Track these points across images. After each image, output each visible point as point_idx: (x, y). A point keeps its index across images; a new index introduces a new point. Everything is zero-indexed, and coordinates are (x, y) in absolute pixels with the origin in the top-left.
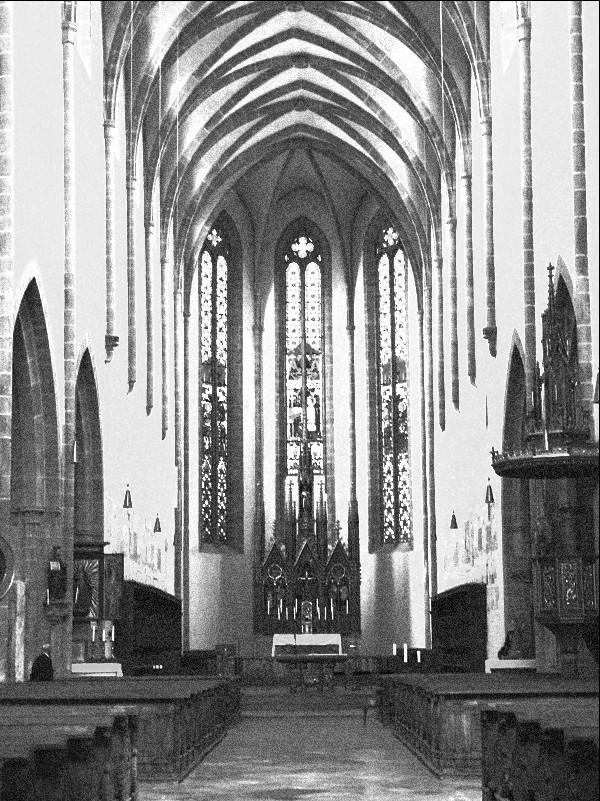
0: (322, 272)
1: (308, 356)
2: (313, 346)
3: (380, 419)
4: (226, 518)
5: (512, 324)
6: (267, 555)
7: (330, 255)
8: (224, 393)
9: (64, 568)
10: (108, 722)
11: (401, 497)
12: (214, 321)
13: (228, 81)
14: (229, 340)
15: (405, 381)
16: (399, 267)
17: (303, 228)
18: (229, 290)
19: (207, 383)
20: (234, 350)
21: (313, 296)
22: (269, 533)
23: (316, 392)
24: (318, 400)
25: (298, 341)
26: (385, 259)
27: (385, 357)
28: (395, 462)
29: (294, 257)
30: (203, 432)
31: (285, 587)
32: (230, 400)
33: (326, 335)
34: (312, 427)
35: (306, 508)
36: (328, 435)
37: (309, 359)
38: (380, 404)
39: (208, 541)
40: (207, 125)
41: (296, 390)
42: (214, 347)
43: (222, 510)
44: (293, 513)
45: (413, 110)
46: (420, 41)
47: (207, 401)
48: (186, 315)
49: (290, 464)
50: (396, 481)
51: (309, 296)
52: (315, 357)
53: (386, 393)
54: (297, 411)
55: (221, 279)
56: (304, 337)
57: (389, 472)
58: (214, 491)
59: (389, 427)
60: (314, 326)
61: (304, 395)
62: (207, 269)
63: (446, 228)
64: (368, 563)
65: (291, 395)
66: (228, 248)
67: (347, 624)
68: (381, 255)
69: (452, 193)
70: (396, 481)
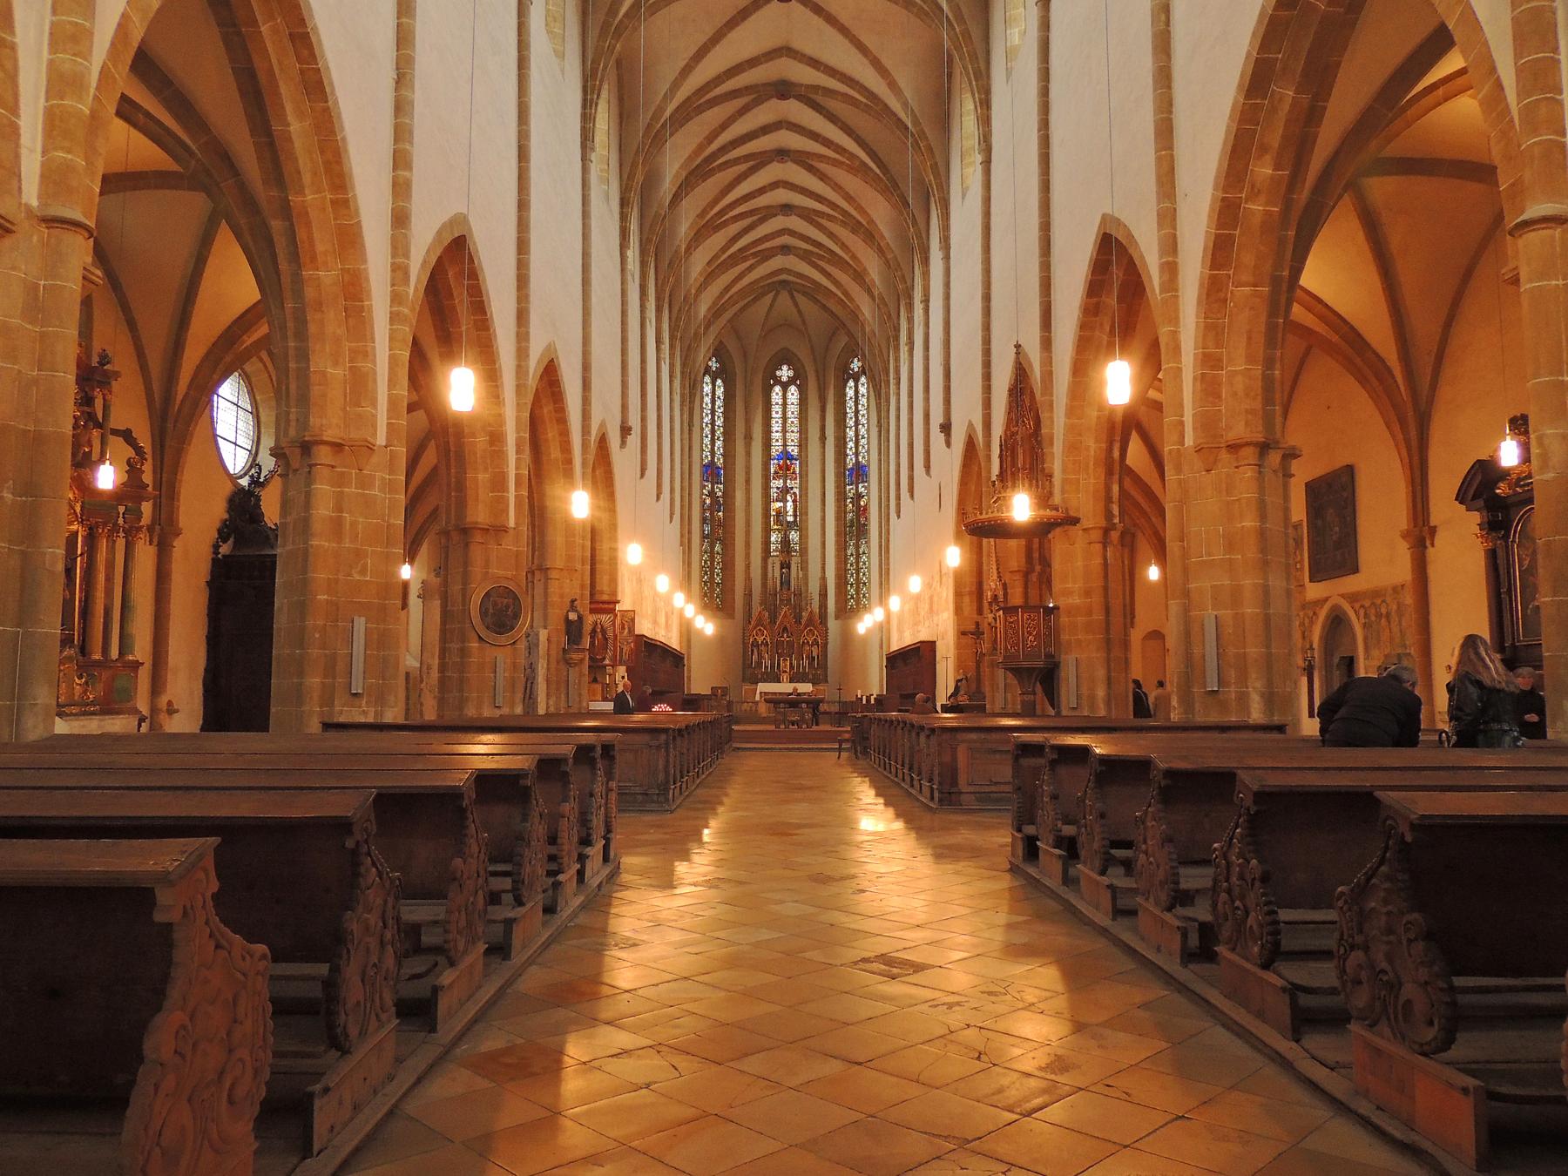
5: (967, 412)
9: (580, 617)
10: (567, 750)
12: (713, 432)
13: (725, 224)
16: (862, 390)
17: (785, 358)
18: (725, 406)
26: (851, 383)
27: (850, 461)
29: (778, 381)
30: (704, 521)
34: (790, 519)
40: (709, 263)
42: (713, 453)
44: (774, 583)
45: (881, 251)
46: (890, 186)
49: (773, 547)
56: (785, 445)
58: (712, 568)
60: (793, 436)
62: (707, 389)
63: (904, 349)
64: (832, 624)
65: (774, 493)
66: (725, 373)
67: (818, 674)
69: (910, 320)
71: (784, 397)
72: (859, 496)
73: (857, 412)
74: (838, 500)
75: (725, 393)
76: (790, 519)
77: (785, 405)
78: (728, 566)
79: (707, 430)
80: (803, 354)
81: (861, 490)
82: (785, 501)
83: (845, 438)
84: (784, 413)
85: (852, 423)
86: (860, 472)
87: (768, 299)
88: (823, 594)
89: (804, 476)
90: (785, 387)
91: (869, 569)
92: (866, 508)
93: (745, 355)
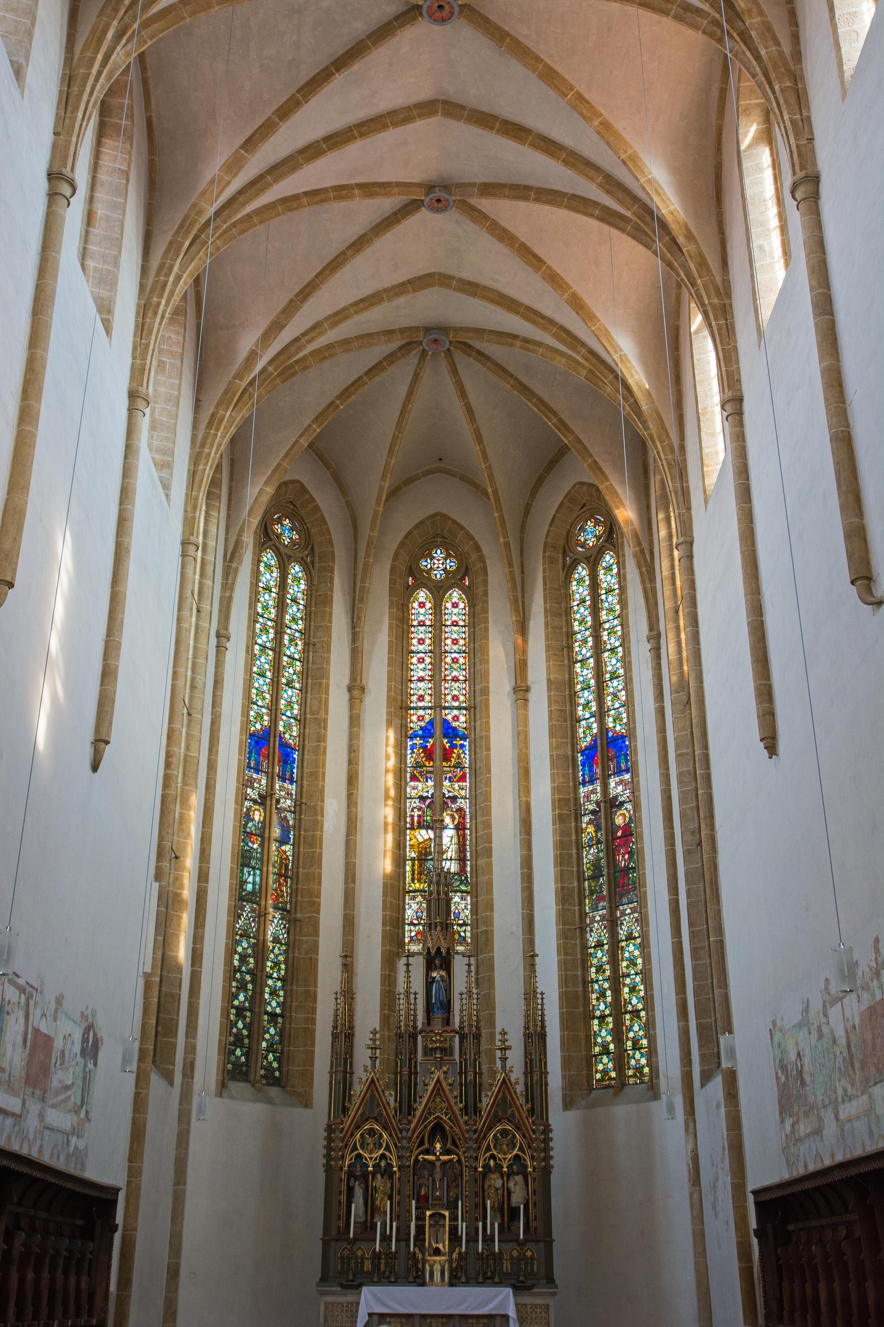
0: (472, 604)
1: (445, 741)
2: (455, 724)
3: (580, 847)
4: (281, 1033)
6: (356, 1101)
7: (486, 574)
8: (289, 794)
12: (277, 667)
14: (303, 704)
15: (627, 771)
16: (607, 580)
17: (439, 533)
18: (309, 616)
19: (257, 771)
20: (312, 719)
21: (455, 642)
22: (362, 1056)
23: (461, 803)
24: (464, 819)
25: (428, 715)
26: (582, 571)
28: (613, 924)
29: (422, 580)
30: (244, 859)
31: (391, 1175)
32: (299, 807)
33: (476, 707)
34: (453, 867)
35: (439, 1006)
36: (483, 878)
37: (447, 745)
38: (578, 817)
39: (235, 1073)
41: (422, 799)
42: (274, 710)
43: (273, 1016)
47: (255, 802)
48: (222, 636)
49: (410, 932)
50: (614, 962)
51: (449, 642)
54: (424, 835)
55: (295, 600)
56: (438, 706)
57: (599, 945)
58: (258, 976)
59: (598, 860)
60: (456, 690)
61: (438, 806)
62: (269, 578)
64: (562, 1122)
70: (614, 962)
72: (612, 804)
73: (597, 626)
74: (560, 819)
75: (310, 593)
76: (453, 867)
77: (438, 626)
78: (300, 971)
79: (264, 662)
80: (473, 520)
81: (616, 788)
82: (438, 826)
83: (571, 683)
84: (437, 640)
85: (586, 652)
86: (612, 751)
87: (404, 369)
88: (535, 1037)
89: (479, 773)
90: (439, 591)
91: (646, 975)
92: (628, 832)
93: (355, 525)
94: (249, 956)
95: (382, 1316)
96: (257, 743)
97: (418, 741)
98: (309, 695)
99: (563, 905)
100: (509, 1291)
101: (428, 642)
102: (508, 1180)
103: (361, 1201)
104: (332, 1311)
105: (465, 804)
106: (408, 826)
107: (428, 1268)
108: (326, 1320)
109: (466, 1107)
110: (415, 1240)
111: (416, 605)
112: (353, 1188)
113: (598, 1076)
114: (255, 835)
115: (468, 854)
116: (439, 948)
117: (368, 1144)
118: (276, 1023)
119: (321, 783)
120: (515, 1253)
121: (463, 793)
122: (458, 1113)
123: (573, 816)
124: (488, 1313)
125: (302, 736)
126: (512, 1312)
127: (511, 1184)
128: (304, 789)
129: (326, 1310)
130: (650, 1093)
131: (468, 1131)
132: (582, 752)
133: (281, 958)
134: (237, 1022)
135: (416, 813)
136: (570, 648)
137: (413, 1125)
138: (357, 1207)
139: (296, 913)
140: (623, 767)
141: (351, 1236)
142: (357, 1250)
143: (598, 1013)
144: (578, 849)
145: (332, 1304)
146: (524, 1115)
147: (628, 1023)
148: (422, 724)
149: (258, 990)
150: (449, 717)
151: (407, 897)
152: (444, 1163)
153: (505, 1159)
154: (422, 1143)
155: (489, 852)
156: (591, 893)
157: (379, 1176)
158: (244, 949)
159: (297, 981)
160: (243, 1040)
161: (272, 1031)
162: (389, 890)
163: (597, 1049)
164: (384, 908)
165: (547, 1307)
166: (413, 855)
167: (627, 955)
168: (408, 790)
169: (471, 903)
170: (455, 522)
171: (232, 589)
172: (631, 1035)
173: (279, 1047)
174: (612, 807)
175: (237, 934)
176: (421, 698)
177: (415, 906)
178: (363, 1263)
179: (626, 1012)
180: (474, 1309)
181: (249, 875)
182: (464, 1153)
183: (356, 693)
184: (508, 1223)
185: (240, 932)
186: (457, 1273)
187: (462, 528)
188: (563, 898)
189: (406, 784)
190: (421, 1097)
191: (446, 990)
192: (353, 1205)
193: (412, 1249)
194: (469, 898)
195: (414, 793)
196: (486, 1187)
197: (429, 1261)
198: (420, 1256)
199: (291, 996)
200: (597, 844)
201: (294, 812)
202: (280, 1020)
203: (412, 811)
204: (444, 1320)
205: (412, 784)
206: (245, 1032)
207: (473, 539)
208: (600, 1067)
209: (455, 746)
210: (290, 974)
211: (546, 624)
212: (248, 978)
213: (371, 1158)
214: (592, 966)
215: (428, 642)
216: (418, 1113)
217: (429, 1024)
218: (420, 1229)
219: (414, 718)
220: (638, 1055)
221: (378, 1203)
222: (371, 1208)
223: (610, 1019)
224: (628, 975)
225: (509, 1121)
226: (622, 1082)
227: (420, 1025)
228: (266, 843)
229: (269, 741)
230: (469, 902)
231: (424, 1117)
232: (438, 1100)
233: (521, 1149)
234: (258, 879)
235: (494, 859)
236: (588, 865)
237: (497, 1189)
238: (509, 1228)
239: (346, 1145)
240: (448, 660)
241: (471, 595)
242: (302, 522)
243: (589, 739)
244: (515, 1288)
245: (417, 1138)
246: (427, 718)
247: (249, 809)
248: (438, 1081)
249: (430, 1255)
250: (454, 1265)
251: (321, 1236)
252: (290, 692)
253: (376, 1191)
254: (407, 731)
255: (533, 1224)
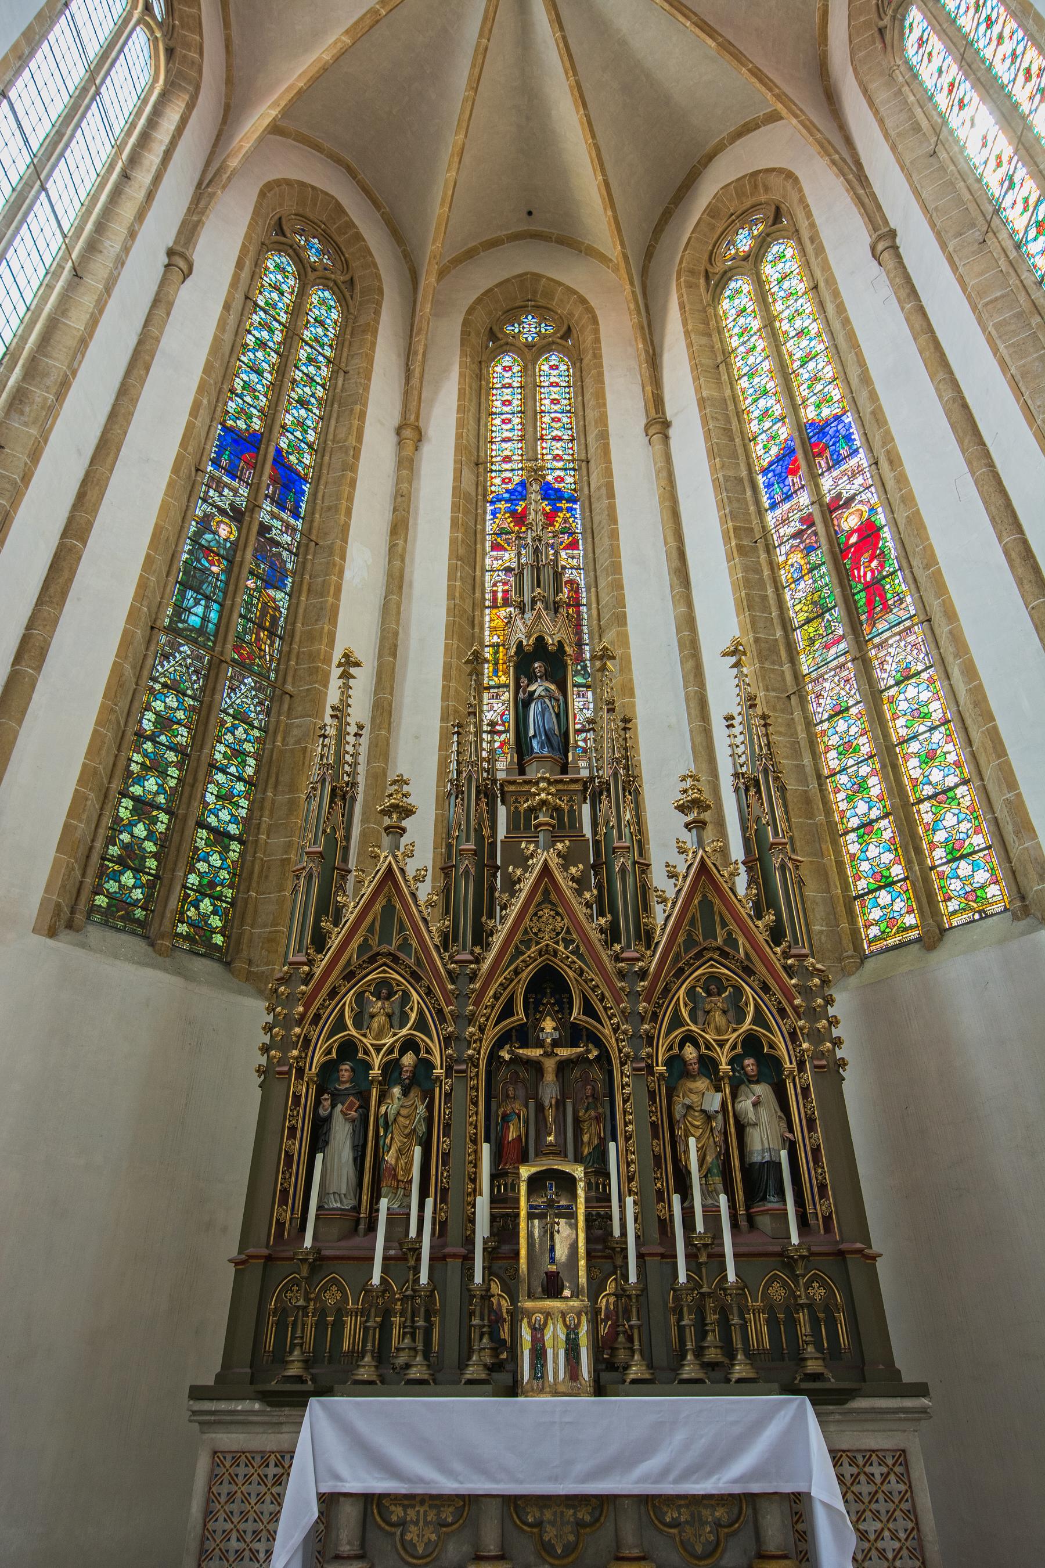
2: (557, 485)
3: (778, 588)
11: (912, 768)
14: (323, 434)
17: (529, 296)
20: (338, 449)
24: (577, 591)
31: (428, 1095)
43: (220, 837)
51: (547, 402)
52: (564, 505)
53: (782, 521)
57: (840, 712)
58: (195, 765)
68: (726, 277)
71: (530, 388)
90: (531, 354)
92: (869, 532)
93: (414, 277)
94: (179, 722)
95: (370, 1501)
96: (235, 441)
97: (502, 505)
98: (333, 422)
99: (761, 662)
100: (798, 1410)
101: (516, 403)
102: (734, 1096)
103: (346, 1154)
104: (233, 1481)
105: (581, 579)
106: (487, 603)
107: (526, 1334)
108: (208, 1514)
109: (614, 926)
110: (490, 1254)
111: (499, 369)
112: (329, 1118)
113: (874, 931)
114: (218, 555)
115: (586, 637)
116: (540, 640)
117: (372, 1016)
118: (226, 849)
119: (343, 518)
120: (777, 1292)
121: (575, 562)
122: (595, 936)
123: (760, 546)
124: (737, 1489)
125: (318, 467)
126: (823, 1487)
127: (745, 1104)
128: (316, 524)
129: (214, 1478)
130: (1023, 924)
131: (622, 975)
132: (765, 471)
133: (248, 747)
134: (132, 824)
135: (500, 588)
136: (729, 366)
137: (486, 966)
138: (336, 1165)
139: (284, 682)
140: (844, 452)
141: (308, 1243)
142: (325, 1289)
143: (854, 822)
144: (777, 589)
145: (237, 1456)
146: (762, 938)
147: (928, 818)
148: (510, 486)
149: (189, 780)
150: (550, 478)
151: (485, 695)
152: (563, 1066)
153: (721, 1044)
154: (508, 1011)
155: (621, 619)
156: (812, 641)
157: (396, 1091)
158: (168, 708)
159: (276, 787)
160: (143, 859)
161: (215, 860)
162: (454, 672)
163: (862, 884)
164: (446, 697)
165: (902, 1456)
166: (495, 639)
167: (903, 706)
168: (488, 561)
169: (595, 701)
170: (549, 279)
171: (203, 213)
172: (940, 836)
173: (229, 893)
174: (831, 512)
175: (155, 680)
176: (507, 459)
177: (498, 707)
178: (339, 1326)
179: (920, 801)
180: (686, 1475)
181: (197, 603)
182: (616, 1029)
183: (407, 433)
184: (748, 1208)
185: (162, 680)
186: (613, 1350)
187: (560, 284)
188: (760, 653)
189: (484, 554)
190: (504, 907)
191: (558, 715)
192: (319, 1157)
193: (478, 1279)
194: (590, 694)
195: (496, 564)
196: (678, 1111)
197: (529, 1314)
198: (505, 1304)
199: (262, 809)
200: (811, 571)
201: (296, 555)
202: (235, 846)
203: (495, 585)
204: (584, 1515)
205: (494, 553)
206: (150, 847)
207: (575, 292)
208: (876, 914)
209: (561, 509)
210: (263, 775)
211: (690, 345)
212: (171, 756)
213: (378, 1043)
214: (828, 749)
215: (516, 403)
216: (497, 941)
217: (522, 771)
218: (504, 1227)
219: (497, 481)
220: (964, 868)
221: (390, 1158)
222: (373, 1174)
223: (884, 823)
224: (915, 737)
225: (724, 954)
226: (934, 934)
227: (501, 775)
228: (236, 569)
229: (259, 448)
230: (591, 699)
231: (515, 947)
232: (546, 912)
233: (759, 1019)
234: (214, 616)
235: (630, 627)
236: (797, 608)
237: (708, 1117)
238: (750, 1219)
239: (317, 1017)
240: (547, 419)
241: (576, 359)
242: (339, 250)
243: (774, 451)
244: (818, 1399)
245: (496, 997)
246: (516, 480)
247: (207, 518)
248: (546, 869)
249: (531, 1296)
250: (603, 1330)
251: (234, 1253)
252: (303, 412)
253: (386, 1126)
254: (485, 496)
255: (818, 1208)
